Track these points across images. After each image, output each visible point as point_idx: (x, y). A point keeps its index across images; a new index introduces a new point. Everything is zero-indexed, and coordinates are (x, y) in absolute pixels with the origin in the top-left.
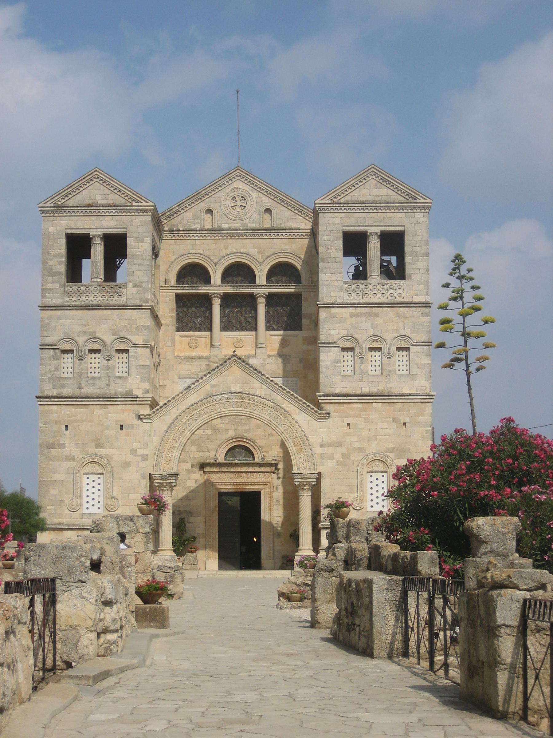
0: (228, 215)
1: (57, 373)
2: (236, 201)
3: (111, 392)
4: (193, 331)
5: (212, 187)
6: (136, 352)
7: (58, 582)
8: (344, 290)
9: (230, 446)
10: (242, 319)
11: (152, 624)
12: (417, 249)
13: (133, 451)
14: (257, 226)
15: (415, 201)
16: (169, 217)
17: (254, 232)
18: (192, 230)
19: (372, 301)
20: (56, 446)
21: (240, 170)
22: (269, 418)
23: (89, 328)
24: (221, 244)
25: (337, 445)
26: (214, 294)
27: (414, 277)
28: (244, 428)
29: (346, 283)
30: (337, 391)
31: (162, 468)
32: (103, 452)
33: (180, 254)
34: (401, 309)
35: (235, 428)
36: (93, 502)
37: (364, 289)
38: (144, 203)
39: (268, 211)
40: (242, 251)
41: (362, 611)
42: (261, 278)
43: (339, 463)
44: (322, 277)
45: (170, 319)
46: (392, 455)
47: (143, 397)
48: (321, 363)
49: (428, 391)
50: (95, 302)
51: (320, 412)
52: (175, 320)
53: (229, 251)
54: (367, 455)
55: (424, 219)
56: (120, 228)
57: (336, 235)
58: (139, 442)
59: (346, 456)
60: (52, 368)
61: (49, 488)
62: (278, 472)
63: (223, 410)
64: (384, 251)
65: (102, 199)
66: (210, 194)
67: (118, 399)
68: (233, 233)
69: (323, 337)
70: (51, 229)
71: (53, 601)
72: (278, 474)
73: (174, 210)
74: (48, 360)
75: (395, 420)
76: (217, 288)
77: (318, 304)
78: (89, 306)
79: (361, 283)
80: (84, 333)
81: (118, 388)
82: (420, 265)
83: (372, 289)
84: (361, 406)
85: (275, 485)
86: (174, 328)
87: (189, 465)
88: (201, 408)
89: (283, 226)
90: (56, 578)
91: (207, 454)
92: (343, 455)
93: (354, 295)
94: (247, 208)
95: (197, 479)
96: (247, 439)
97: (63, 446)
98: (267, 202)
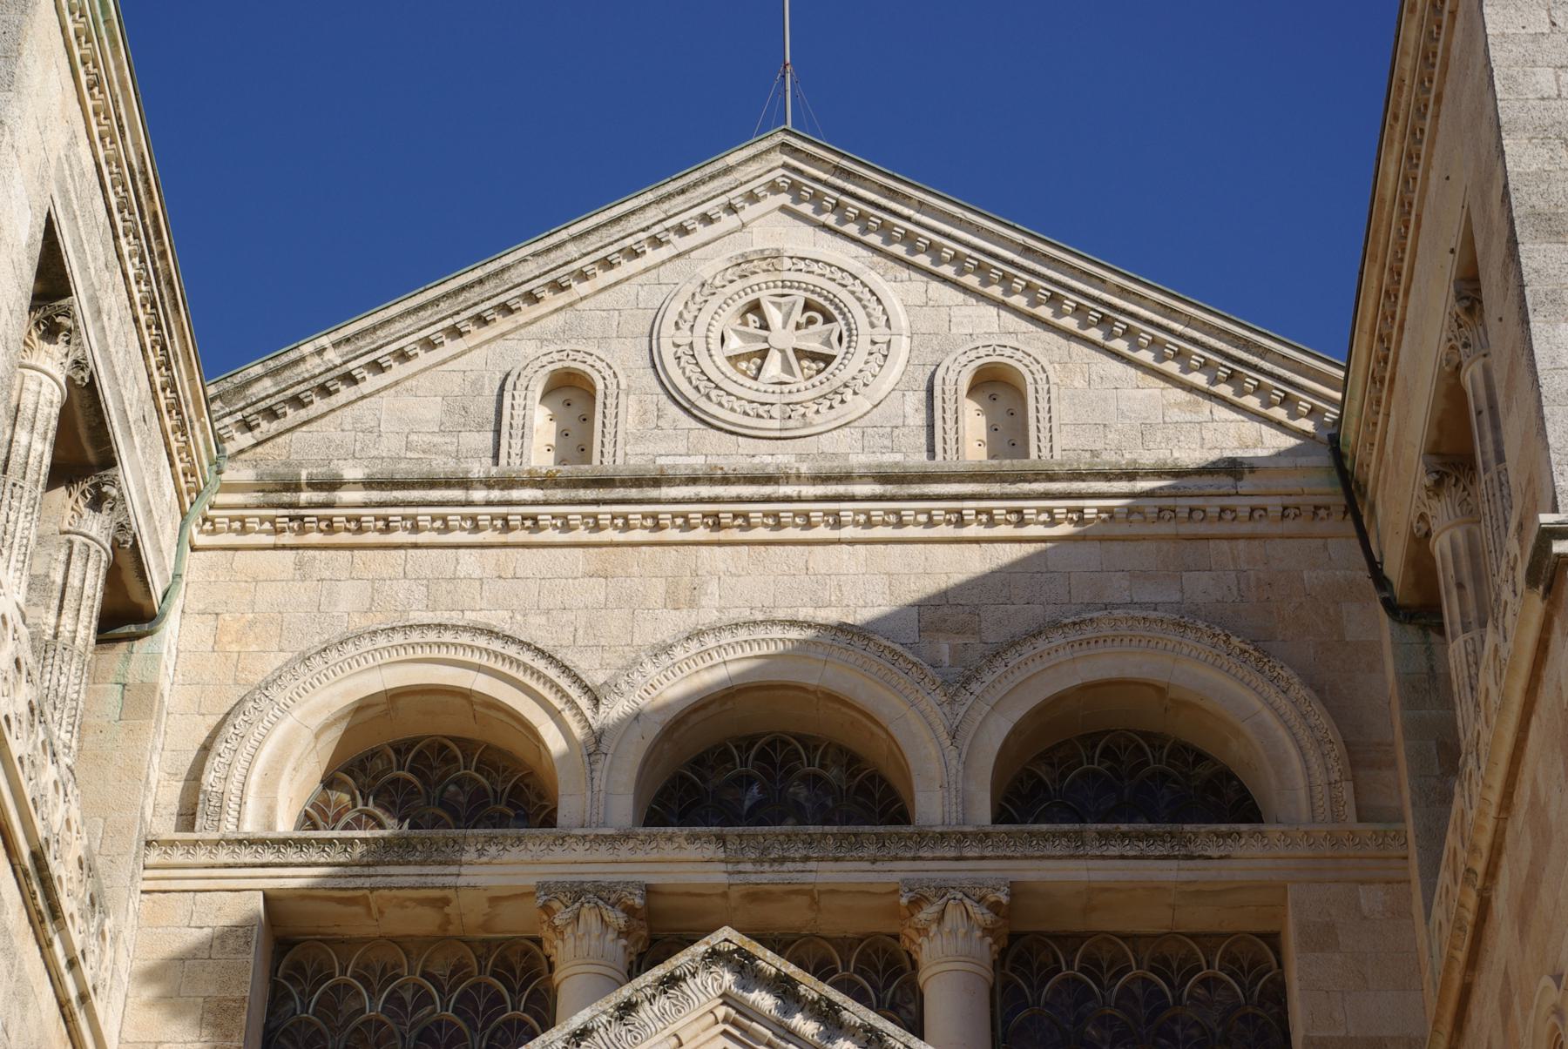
0: (702, 402)
2: (765, 326)
5: (594, 241)
14: (917, 459)
16: (271, 414)
17: (890, 489)
18: (431, 483)
21: (794, 151)
33: (335, 634)
40: (803, 614)
68: (739, 500)
73: (313, 365)
76: (603, 853)
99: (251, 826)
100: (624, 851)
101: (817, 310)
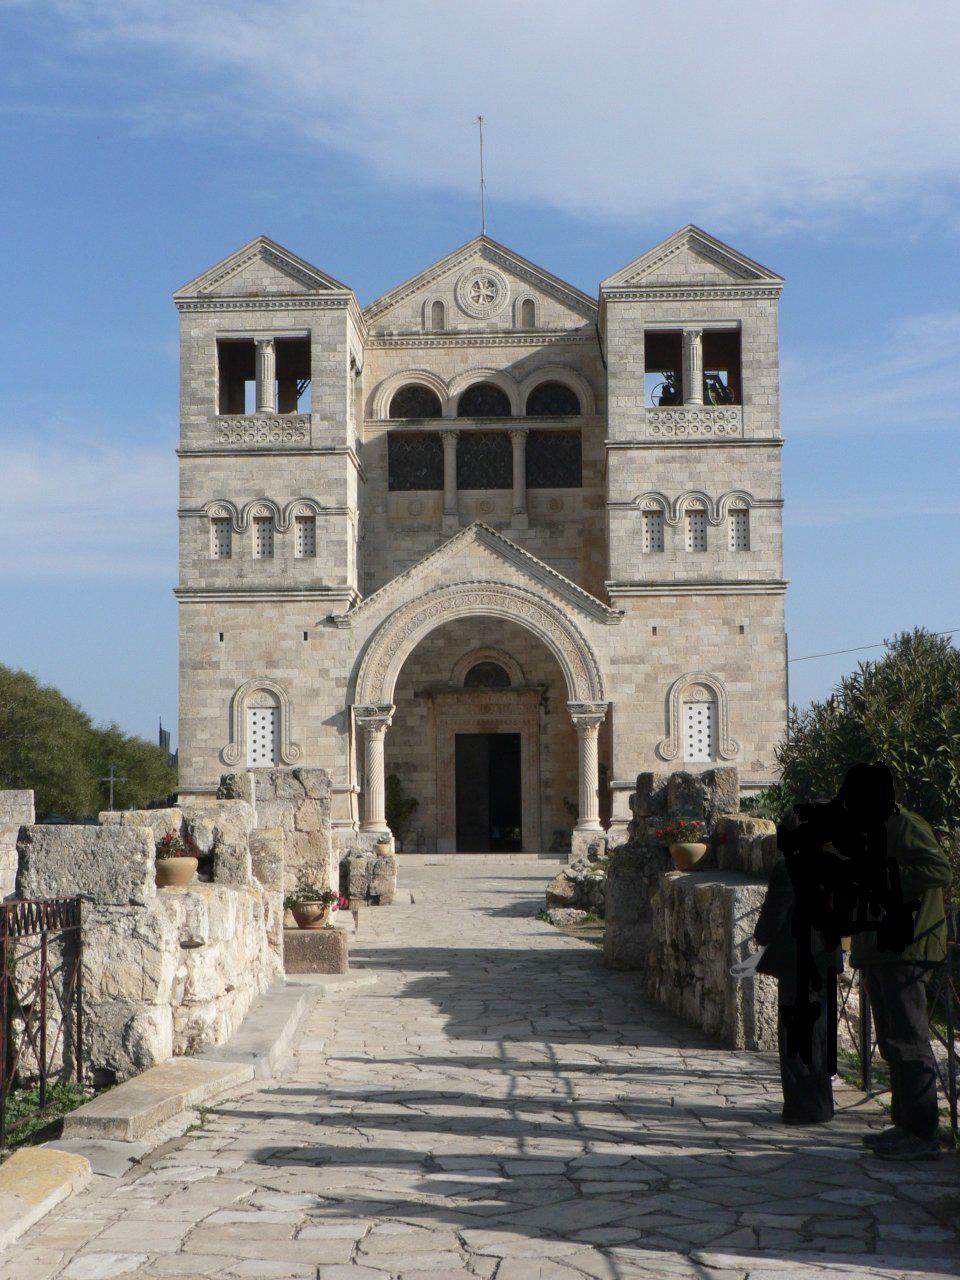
1: (206, 553)
2: (479, 288)
3: (288, 582)
4: (416, 489)
6: (326, 521)
7: (86, 906)
8: (647, 421)
9: (473, 664)
10: (490, 470)
11: (315, 966)
12: (762, 357)
13: (324, 673)
15: (757, 281)
19: (690, 438)
20: (207, 666)
22: (531, 620)
23: (255, 485)
24: (458, 353)
25: (637, 661)
26: (446, 431)
27: (756, 399)
29: (650, 411)
30: (636, 579)
31: (367, 699)
32: (278, 673)
34: (737, 450)
36: (263, 751)
37: (678, 420)
38: (336, 291)
39: (528, 303)
40: (489, 365)
41: (708, 953)
42: (518, 406)
43: (640, 688)
44: (612, 401)
45: (380, 472)
46: (721, 676)
47: (338, 590)
48: (612, 535)
49: (777, 577)
50: (264, 444)
51: (610, 610)
52: (387, 473)
53: (470, 365)
54: (683, 676)
55: (772, 310)
56: (301, 330)
57: (633, 335)
58: (333, 658)
59: (651, 678)
60: (199, 545)
61: (195, 730)
63: (461, 608)
64: (709, 362)
65: (272, 284)
67: (300, 593)
69: (614, 494)
70: (194, 333)
71: (73, 947)
72: (546, 707)
74: (191, 533)
75: (726, 622)
77: (606, 444)
78: (254, 451)
79: (674, 411)
80: (246, 491)
81: (301, 575)
82: (765, 381)
83: (691, 419)
84: (673, 600)
85: (542, 723)
86: (386, 484)
87: (410, 694)
88: (426, 606)
89: (551, 326)
90: (78, 899)
91: (439, 677)
92: (647, 675)
93: (663, 430)
94: (497, 300)
97: (215, 665)
98: (526, 290)
99: (383, 417)
100: (456, 422)
101: (491, 284)
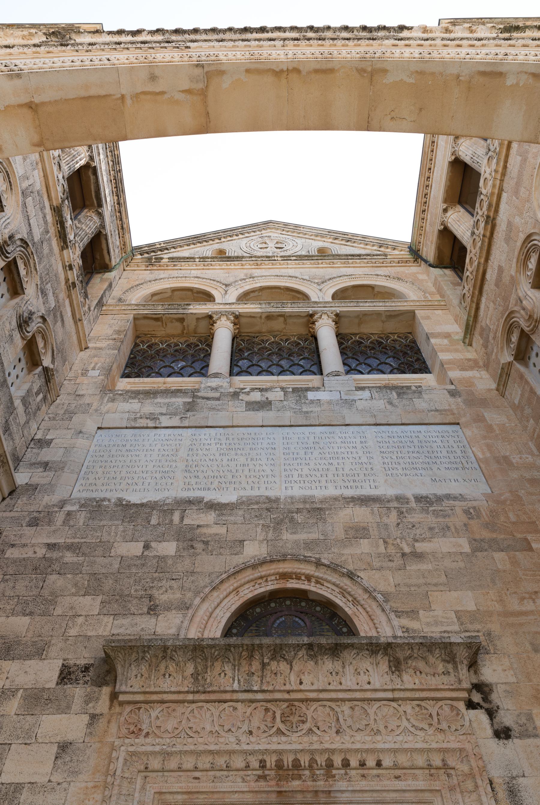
28: (302, 536)
35: (270, 535)
62: (486, 699)
66: (223, 240)
95: (70, 737)
96: (318, 564)
